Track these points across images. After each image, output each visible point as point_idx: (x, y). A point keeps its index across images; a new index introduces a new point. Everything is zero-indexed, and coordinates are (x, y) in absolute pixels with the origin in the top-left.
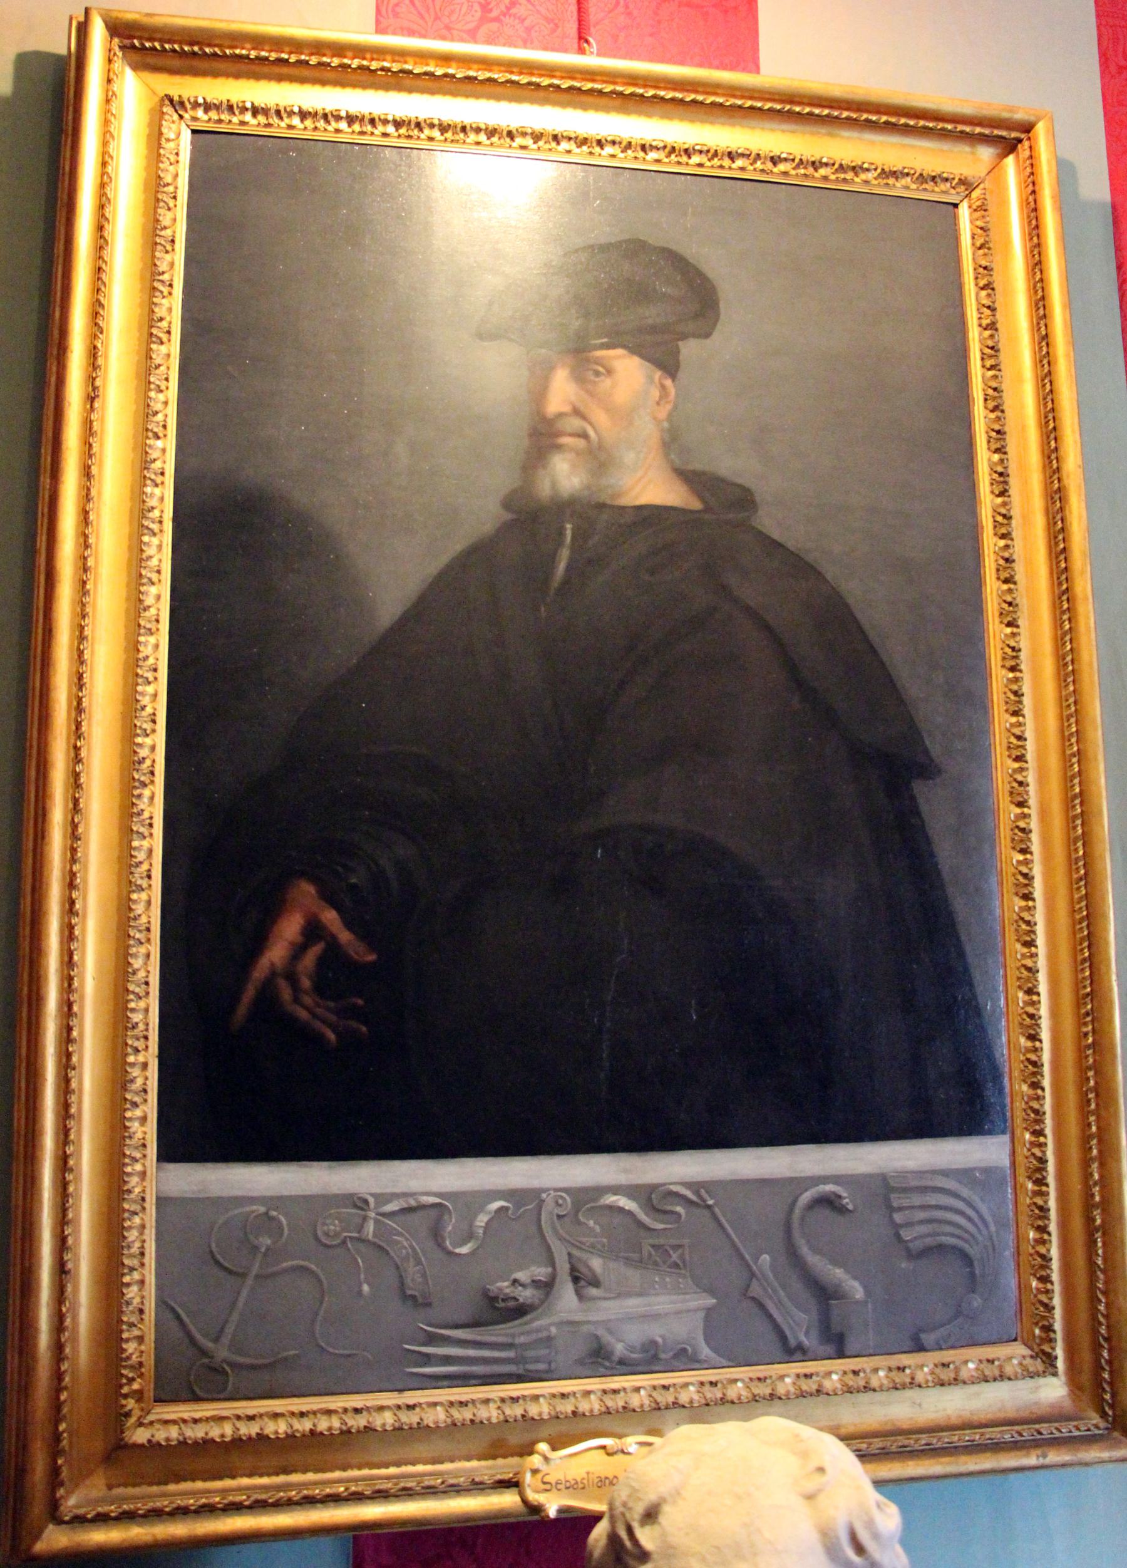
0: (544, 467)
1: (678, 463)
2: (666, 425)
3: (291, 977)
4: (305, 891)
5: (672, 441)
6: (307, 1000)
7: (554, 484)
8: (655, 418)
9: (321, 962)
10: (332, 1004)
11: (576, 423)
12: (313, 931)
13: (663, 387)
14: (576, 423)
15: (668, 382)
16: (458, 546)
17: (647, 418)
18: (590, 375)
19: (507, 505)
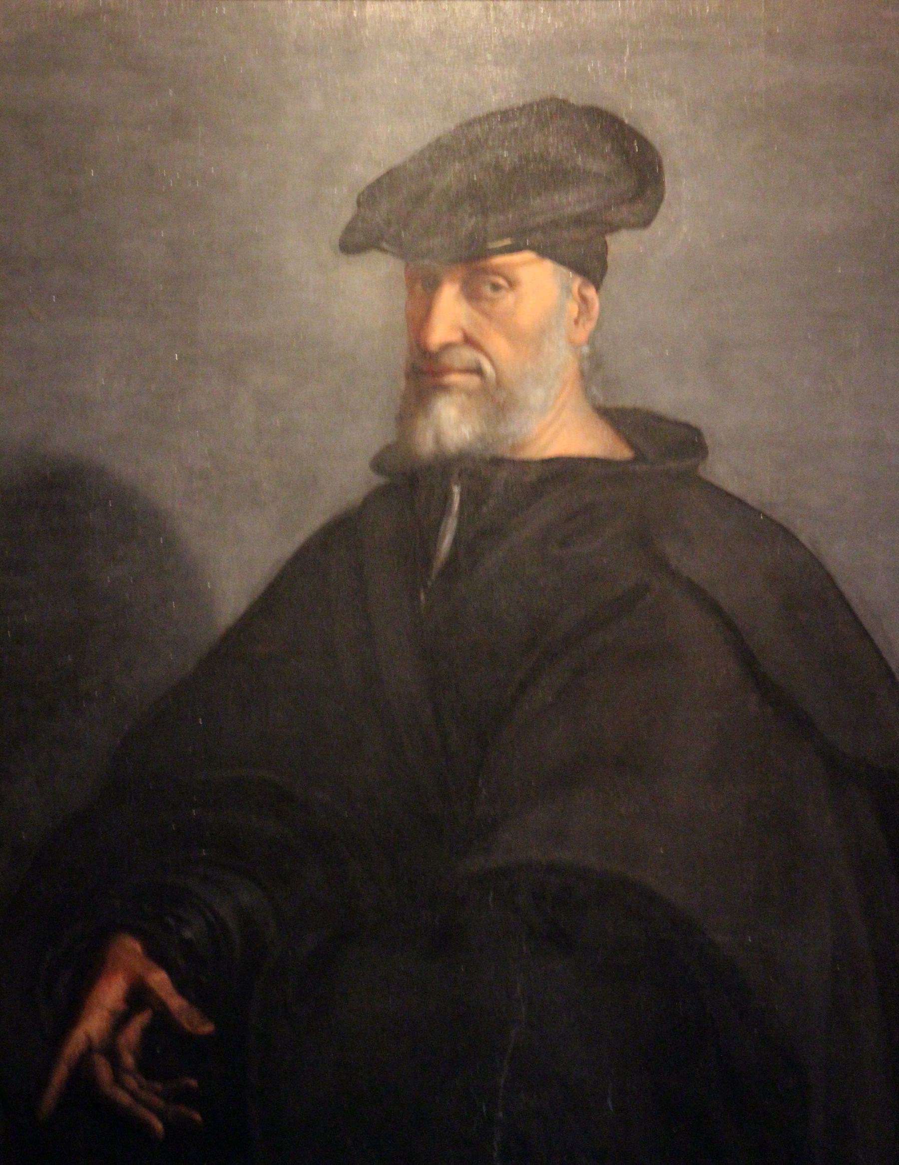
0: (427, 415)
1: (601, 400)
2: (586, 350)
3: (111, 1052)
4: (130, 949)
5: (594, 369)
6: (131, 1082)
7: (437, 440)
8: (571, 342)
9: (148, 1032)
10: (159, 1086)
11: (467, 355)
12: (138, 996)
13: (584, 299)
14: (467, 355)
15: (591, 292)
16: (314, 521)
17: (562, 343)
18: (487, 290)
19: (378, 465)
